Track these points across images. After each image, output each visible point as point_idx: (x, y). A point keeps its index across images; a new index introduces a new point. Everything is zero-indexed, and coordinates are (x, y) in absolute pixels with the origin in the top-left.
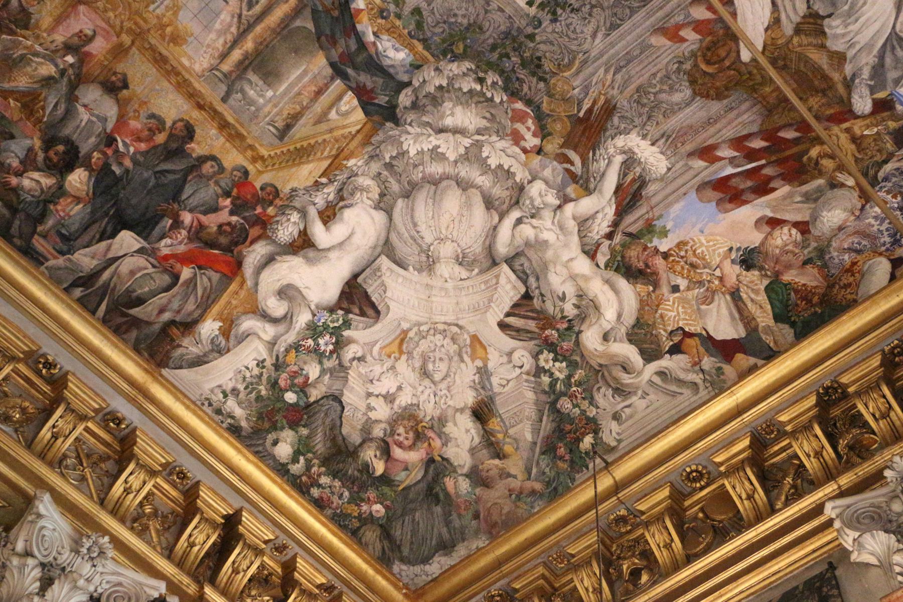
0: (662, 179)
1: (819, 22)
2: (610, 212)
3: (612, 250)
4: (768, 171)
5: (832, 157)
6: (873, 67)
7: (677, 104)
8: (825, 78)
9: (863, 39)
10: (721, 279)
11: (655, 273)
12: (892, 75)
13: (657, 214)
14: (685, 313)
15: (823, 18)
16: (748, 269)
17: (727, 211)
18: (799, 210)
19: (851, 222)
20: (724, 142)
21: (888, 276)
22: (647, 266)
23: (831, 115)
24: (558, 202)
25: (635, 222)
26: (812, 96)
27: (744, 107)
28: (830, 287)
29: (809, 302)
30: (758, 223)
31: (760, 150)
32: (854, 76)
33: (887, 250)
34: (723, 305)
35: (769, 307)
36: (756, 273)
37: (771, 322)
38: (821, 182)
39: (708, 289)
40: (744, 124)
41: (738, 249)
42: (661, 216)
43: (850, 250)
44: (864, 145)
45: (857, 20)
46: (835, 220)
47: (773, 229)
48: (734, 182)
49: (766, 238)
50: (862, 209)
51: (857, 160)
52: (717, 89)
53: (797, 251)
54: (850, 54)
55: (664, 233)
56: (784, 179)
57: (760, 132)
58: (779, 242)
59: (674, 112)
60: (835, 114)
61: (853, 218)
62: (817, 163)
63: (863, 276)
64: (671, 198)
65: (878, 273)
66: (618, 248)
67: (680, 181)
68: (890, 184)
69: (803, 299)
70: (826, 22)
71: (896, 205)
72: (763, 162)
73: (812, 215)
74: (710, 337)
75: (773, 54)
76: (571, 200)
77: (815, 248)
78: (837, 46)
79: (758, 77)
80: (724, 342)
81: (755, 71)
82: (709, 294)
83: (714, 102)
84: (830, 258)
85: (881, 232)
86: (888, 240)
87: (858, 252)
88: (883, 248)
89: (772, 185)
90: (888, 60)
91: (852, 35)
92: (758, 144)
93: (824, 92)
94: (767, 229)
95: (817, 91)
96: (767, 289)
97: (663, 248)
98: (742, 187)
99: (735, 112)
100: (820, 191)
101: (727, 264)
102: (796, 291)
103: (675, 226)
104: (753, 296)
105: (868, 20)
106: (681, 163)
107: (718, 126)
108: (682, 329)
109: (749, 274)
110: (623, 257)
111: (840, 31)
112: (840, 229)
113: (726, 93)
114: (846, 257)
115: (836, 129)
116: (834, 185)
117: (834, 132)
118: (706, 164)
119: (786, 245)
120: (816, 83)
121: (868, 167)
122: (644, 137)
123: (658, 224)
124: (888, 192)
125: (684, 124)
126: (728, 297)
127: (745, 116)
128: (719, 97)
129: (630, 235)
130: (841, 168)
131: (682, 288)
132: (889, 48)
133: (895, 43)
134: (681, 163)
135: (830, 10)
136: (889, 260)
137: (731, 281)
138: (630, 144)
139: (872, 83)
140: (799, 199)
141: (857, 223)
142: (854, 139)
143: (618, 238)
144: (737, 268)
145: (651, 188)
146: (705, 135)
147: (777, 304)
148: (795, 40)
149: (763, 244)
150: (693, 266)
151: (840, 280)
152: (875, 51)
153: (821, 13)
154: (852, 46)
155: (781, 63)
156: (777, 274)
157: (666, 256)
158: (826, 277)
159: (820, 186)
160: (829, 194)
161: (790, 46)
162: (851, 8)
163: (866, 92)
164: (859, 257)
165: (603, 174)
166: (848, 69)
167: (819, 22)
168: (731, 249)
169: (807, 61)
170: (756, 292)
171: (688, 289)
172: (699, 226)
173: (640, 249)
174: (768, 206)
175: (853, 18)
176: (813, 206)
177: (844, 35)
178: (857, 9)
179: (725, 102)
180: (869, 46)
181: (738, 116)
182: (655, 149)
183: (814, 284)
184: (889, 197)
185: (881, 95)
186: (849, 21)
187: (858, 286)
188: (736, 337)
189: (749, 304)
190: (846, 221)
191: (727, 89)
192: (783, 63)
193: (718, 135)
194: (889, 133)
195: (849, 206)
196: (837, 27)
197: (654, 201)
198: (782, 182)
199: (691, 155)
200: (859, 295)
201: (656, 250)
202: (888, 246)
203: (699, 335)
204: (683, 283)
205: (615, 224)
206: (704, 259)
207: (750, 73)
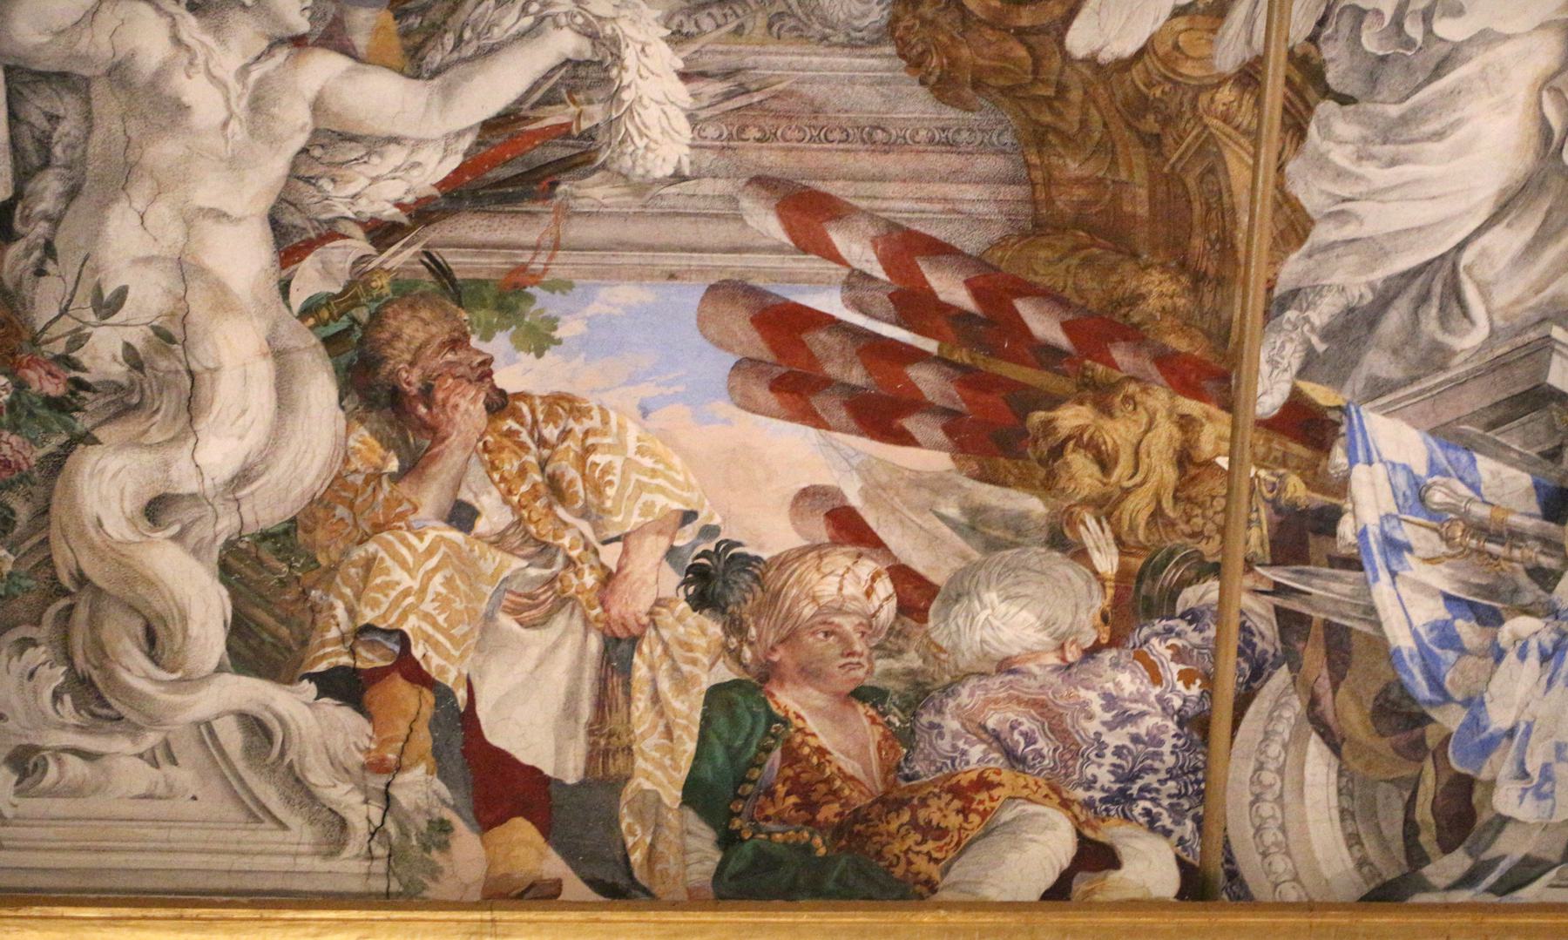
0: (642, 187)
1: (1311, 94)
2: (435, 167)
3: (360, 277)
4: (926, 380)
5: (1105, 463)
6: (1350, 310)
7: (825, 22)
8: (1225, 246)
9: (1375, 219)
10: (608, 579)
11: (435, 432)
12: (1377, 363)
13: (558, 272)
14: (444, 602)
15: (1327, 92)
16: (700, 602)
17: (749, 405)
18: (933, 540)
19: (1043, 668)
20: (871, 215)
21: (1051, 878)
22: (427, 393)
23: (1176, 354)
24: (302, 25)
25: (481, 247)
26: (1164, 268)
27: (987, 164)
28: (889, 803)
29: (809, 806)
30: (808, 496)
31: (946, 308)
32: (1295, 293)
33: (1089, 804)
34: (566, 656)
35: (691, 746)
36: (715, 629)
37: (672, 795)
38: (1034, 506)
39: (551, 581)
40: (953, 209)
41: (709, 531)
42: (564, 286)
43: (996, 738)
44: (1199, 491)
45: (1393, 162)
46: (1007, 634)
47: (835, 543)
48: (819, 340)
49: (802, 553)
50: (1091, 652)
51: (1157, 513)
52: (953, 63)
53: (859, 647)
54: (1323, 233)
55: (540, 340)
56: (949, 431)
57: (979, 261)
58: (828, 589)
59: (801, 34)
60: (1187, 358)
61: (1052, 659)
62: (1058, 451)
63: (987, 833)
64: (630, 258)
65: (1033, 850)
66: (382, 283)
67: (684, 231)
68: (1195, 638)
69: (796, 786)
70: (1327, 107)
71: (1177, 703)
72: (931, 346)
73: (958, 577)
74: (469, 719)
75: (1150, 85)
76: (347, 50)
77: (911, 672)
78: (1311, 193)
79: (1073, 116)
80: (502, 760)
81: (1075, 95)
82: (547, 596)
83: (922, 92)
84: (932, 726)
85: (1102, 746)
86: (1105, 778)
87: (1014, 759)
88: (1081, 794)
89: (910, 424)
90: (1393, 321)
91: (1362, 188)
92: (950, 288)
93: (1198, 278)
94: (822, 533)
95: (1183, 266)
96: (716, 694)
97: (507, 378)
98: (832, 369)
99: (955, 161)
100: (1017, 526)
101: (652, 549)
102: (791, 756)
103: (584, 343)
104: (665, 685)
105: (1418, 181)
106: (722, 186)
107: (891, 163)
108: (404, 640)
109: (694, 618)
110: (377, 318)
111: (1340, 156)
112: (1006, 666)
113: (968, 92)
114: (976, 752)
115: (1160, 398)
116: (1061, 540)
117: (1151, 402)
118: (785, 239)
119: (840, 611)
120: (1197, 243)
121: (1171, 554)
122: (677, 38)
123: (544, 301)
124: (1179, 655)
125: (806, 89)
126: (594, 643)
127: (971, 192)
128: (944, 88)
129: (441, 272)
130: (1106, 506)
131: (481, 526)
132: (1414, 289)
133: (1437, 288)
134: (722, 186)
135: (1351, 87)
136: (1079, 834)
137: (633, 603)
138: (625, 28)
139: (1321, 347)
140: (953, 511)
141: (1055, 679)
142: (1185, 459)
143: (401, 257)
144: (670, 581)
145: (594, 191)
146: (838, 159)
147: (720, 756)
148: (1226, 94)
149: (782, 562)
150: (556, 488)
151: (924, 803)
152: (1379, 275)
153: (1331, 77)
154: (1340, 217)
155: (1150, 124)
156: (768, 673)
157: (500, 404)
158: (892, 770)
159: (1025, 515)
160: (1036, 554)
161: (1204, 100)
162: (1404, 120)
163: (1292, 357)
164: (1006, 776)
165: (492, 51)
166: (1293, 269)
167: (1311, 94)
168: (689, 516)
169: (1214, 167)
170: (682, 683)
171: (499, 541)
172: (648, 391)
173: (441, 331)
174: (865, 470)
175: (1389, 149)
176: (976, 556)
177: (1340, 174)
178: (1415, 133)
179: (951, 114)
180: (1376, 248)
181: (953, 176)
182: (681, 92)
183: (851, 767)
184: (1175, 668)
185: (1320, 394)
186: (1376, 149)
187: (962, 849)
188: (548, 771)
189: (641, 702)
190: (1033, 654)
191: (977, 85)
192: (1156, 129)
193: (866, 188)
194: (1273, 503)
195: (1065, 621)
196: (1341, 142)
197: (576, 231)
198: (939, 436)
199: (762, 182)
200: (953, 875)
201: (484, 371)
202: (1098, 795)
203: (443, 694)
204: (493, 514)
205: (423, 213)
206: (598, 490)
207: (1062, 90)
